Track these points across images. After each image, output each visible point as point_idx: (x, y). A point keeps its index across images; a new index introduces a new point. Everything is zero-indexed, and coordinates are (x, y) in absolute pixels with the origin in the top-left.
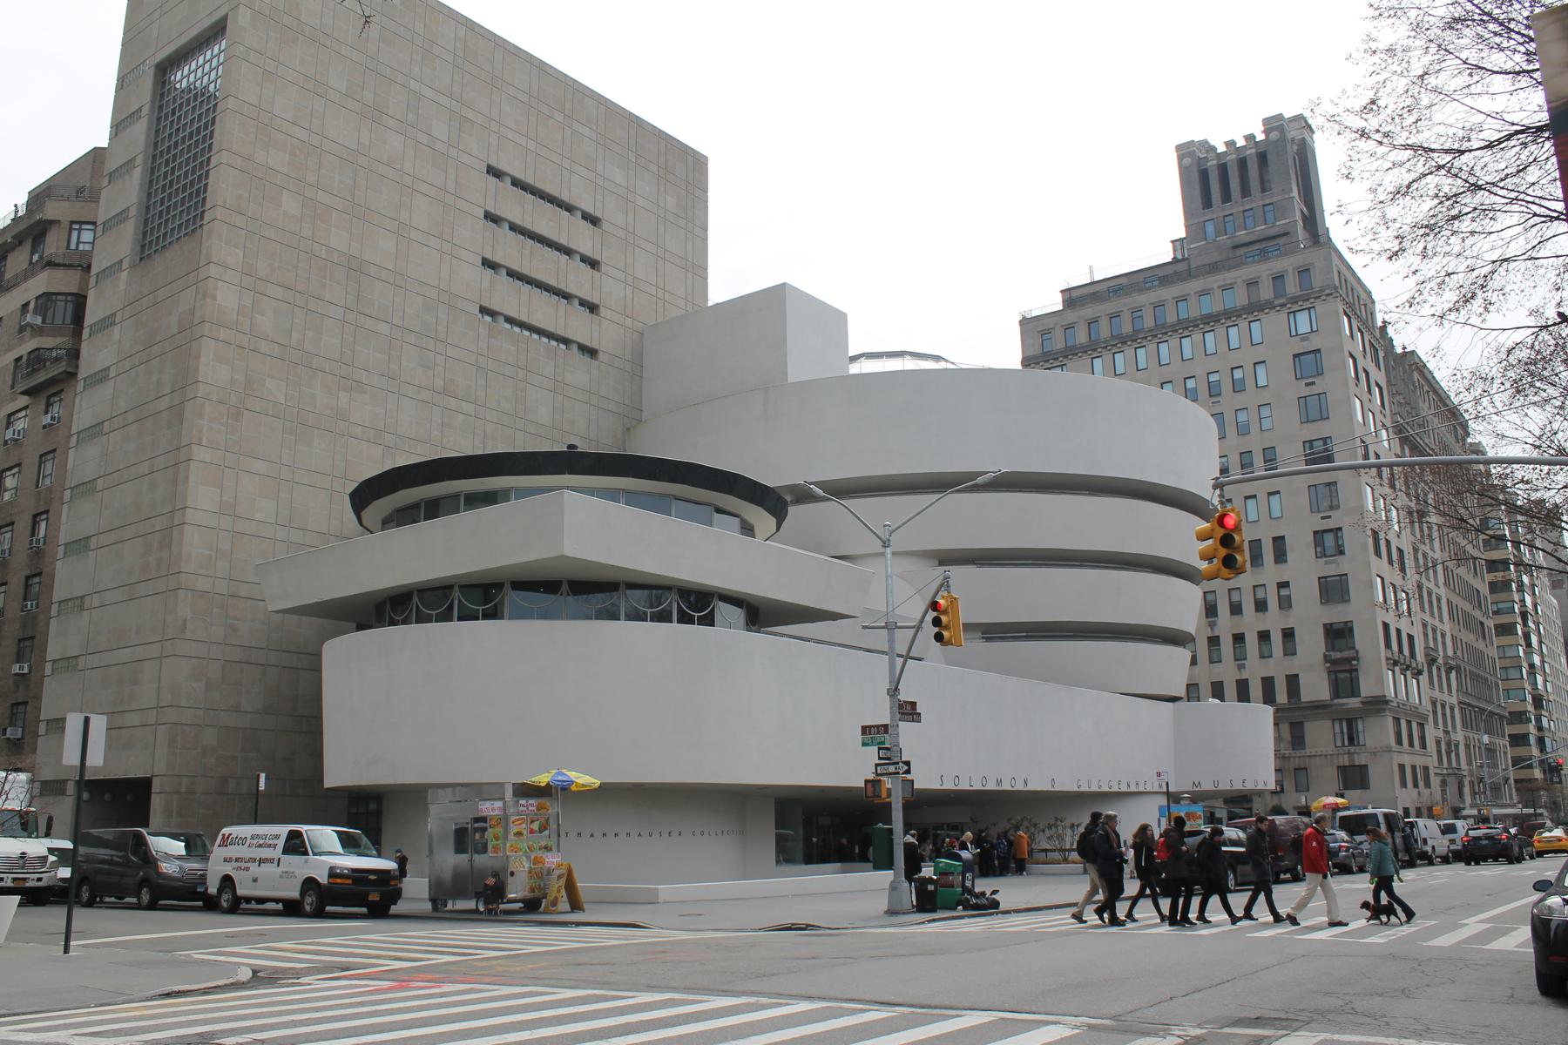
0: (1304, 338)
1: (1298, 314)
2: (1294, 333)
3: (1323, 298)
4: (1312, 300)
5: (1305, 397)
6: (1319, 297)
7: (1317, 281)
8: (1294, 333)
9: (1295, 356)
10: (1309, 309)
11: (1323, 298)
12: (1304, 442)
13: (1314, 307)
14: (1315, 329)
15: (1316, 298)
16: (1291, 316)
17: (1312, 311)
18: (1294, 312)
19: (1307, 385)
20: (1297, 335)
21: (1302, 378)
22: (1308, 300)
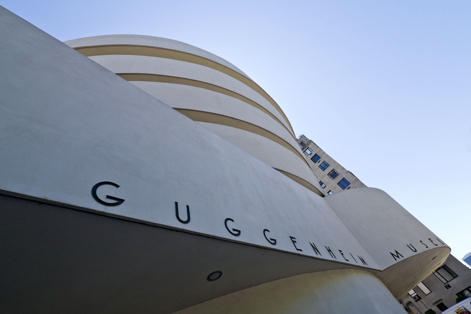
0: (311, 154)
1: (306, 151)
2: (307, 155)
3: (309, 144)
4: (307, 146)
5: (320, 165)
6: (308, 144)
7: (305, 142)
8: (307, 155)
9: (311, 159)
10: (308, 148)
11: (309, 144)
12: (328, 175)
13: (308, 147)
14: (312, 151)
15: (307, 145)
16: (305, 153)
17: (309, 148)
18: (305, 151)
19: (318, 162)
20: (308, 155)
21: (316, 162)
22: (306, 147)
